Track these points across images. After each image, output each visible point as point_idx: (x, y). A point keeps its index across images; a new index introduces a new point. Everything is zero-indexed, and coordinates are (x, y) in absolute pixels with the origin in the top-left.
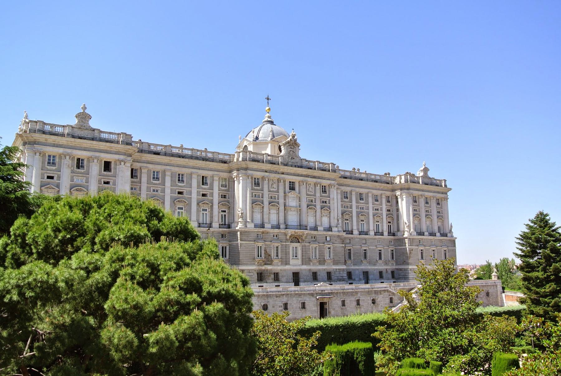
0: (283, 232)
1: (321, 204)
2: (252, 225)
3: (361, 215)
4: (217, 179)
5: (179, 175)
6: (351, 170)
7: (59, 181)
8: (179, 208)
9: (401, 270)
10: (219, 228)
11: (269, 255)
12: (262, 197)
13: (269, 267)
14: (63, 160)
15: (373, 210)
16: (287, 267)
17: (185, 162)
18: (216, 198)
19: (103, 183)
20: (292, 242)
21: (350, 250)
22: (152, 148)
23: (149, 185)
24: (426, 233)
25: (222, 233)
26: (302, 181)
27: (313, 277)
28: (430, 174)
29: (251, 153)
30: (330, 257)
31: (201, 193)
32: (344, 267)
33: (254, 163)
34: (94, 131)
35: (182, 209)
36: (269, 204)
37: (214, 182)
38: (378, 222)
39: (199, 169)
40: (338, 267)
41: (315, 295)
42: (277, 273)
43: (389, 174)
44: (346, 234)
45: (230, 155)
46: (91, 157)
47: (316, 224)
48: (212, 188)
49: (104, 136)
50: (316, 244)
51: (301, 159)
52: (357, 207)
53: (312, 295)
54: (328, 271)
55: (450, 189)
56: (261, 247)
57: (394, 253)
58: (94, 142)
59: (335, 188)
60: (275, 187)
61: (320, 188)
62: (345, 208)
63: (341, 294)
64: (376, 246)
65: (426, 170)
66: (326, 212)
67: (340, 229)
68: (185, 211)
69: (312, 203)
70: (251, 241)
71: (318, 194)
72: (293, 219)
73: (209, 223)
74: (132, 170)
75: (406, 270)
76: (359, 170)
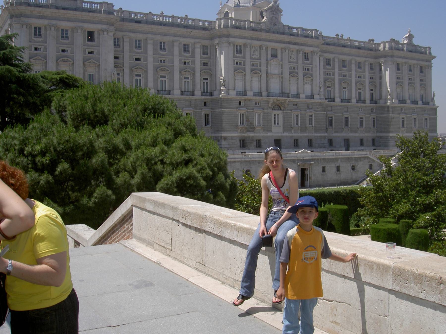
0: (265, 99)
1: (304, 71)
2: (235, 92)
3: (344, 83)
4: (199, 46)
5: (161, 43)
6: (334, 36)
7: (46, 53)
8: (162, 77)
9: (381, 137)
10: (202, 96)
11: (251, 123)
12: (244, 65)
13: (251, 134)
14: (48, 32)
15: (355, 78)
16: (269, 134)
18: (198, 66)
19: (87, 53)
20: (274, 110)
21: (331, 117)
22: (133, 16)
23: (156, 56)
24: (408, 102)
25: (205, 101)
26: (285, 49)
27: (294, 144)
28: (415, 42)
29: (232, 20)
30: (311, 124)
31: (183, 61)
32: (326, 134)
33: (235, 30)
35: (165, 77)
36: (251, 72)
38: (361, 89)
39: (181, 37)
40: (319, 135)
41: (297, 162)
42: (259, 140)
43: (373, 40)
44: (329, 101)
45: (211, 22)
46: (75, 28)
47: (298, 91)
48: (193, 56)
49: (86, 6)
50: (298, 112)
51: (284, 26)
52: (340, 75)
53: (293, 161)
55: (434, 57)
56: (243, 114)
57: (376, 121)
58: (78, 13)
59: (318, 55)
60: (257, 54)
61: (303, 55)
62: (327, 75)
63: (322, 161)
64: (358, 114)
65: (410, 37)
66: (308, 79)
67: (322, 97)
68: (168, 80)
69: (294, 71)
71: (300, 62)
72: (275, 86)
73: (191, 91)
74: (115, 39)
75: (387, 137)
76: (342, 36)
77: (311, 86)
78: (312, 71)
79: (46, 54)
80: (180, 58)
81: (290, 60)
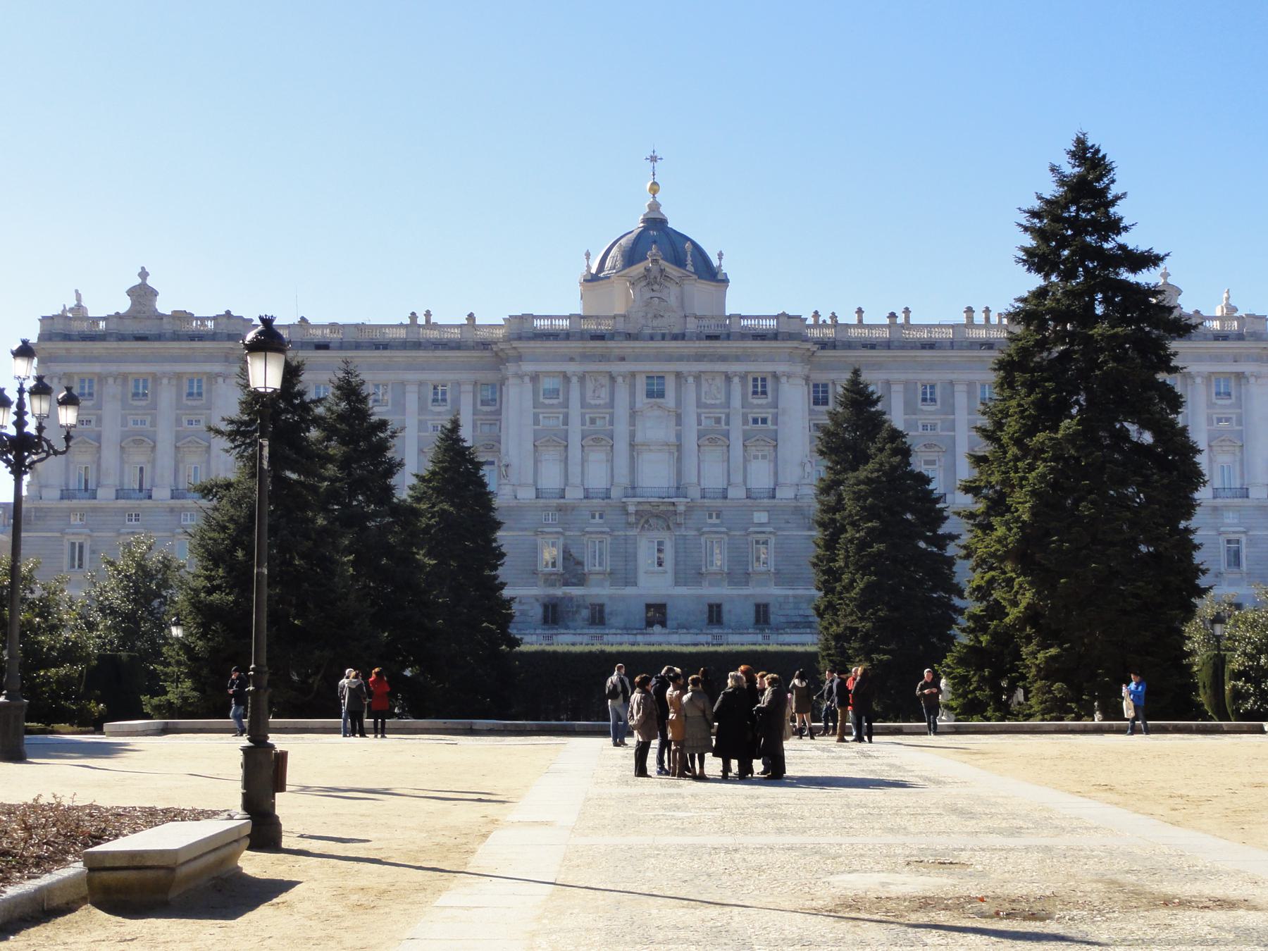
4: (469, 388)
6: (887, 322)
12: (566, 423)
16: (629, 591)
17: (385, 357)
20: (648, 530)
34: (162, 319)
37: (463, 397)
39: (424, 369)
40: (790, 592)
42: (602, 606)
47: (729, 481)
54: (759, 601)
60: (603, 395)
61: (744, 385)
70: (526, 529)
71: (736, 402)
77: (772, 465)
78: (775, 422)
79: (100, 432)
80: (422, 417)
81: (703, 400)
